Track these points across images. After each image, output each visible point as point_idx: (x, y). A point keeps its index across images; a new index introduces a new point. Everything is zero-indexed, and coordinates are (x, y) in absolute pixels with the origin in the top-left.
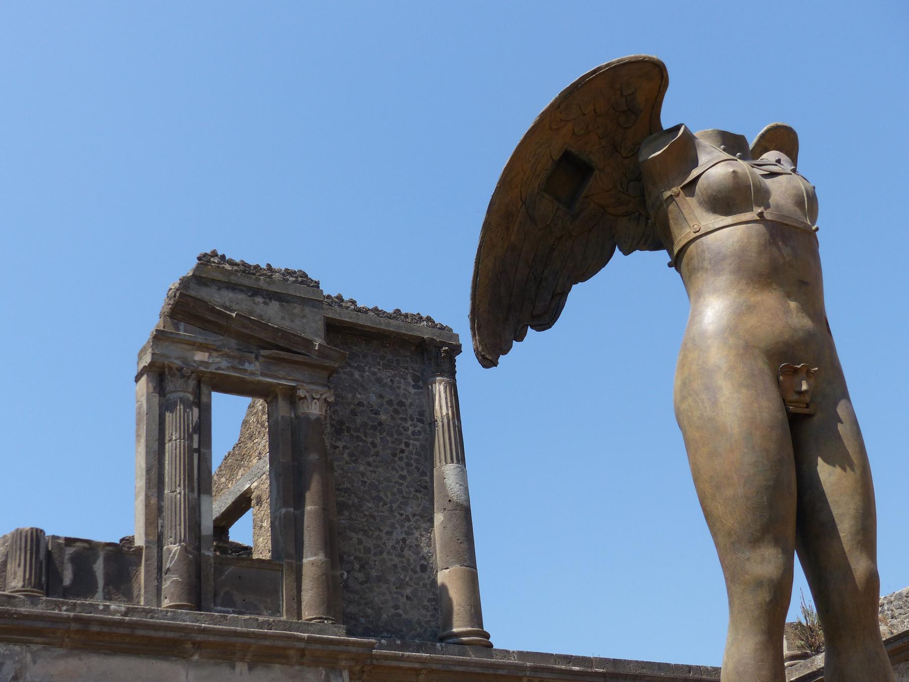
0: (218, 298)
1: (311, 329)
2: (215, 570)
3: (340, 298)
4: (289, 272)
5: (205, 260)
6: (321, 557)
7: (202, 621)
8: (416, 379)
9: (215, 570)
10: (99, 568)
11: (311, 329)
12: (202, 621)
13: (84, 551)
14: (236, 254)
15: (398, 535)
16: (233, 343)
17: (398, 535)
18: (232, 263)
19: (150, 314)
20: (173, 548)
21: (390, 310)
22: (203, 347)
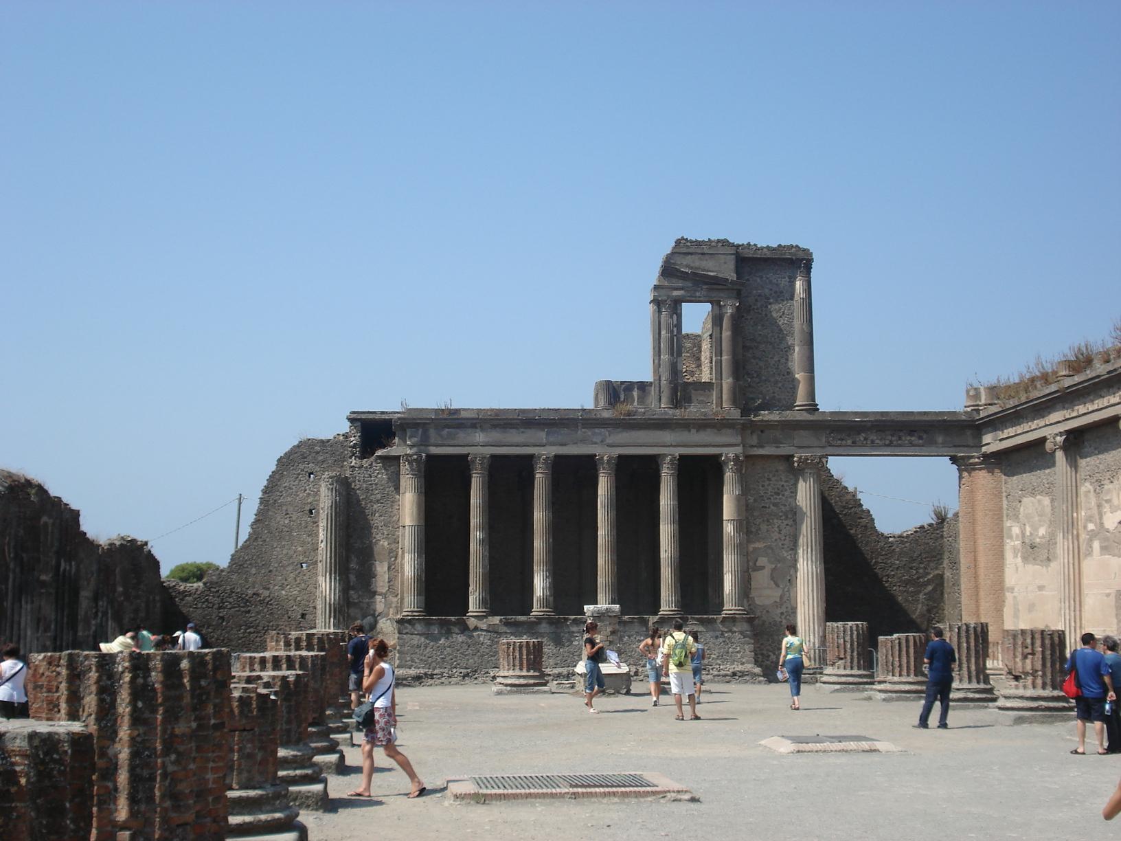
0: (684, 264)
1: (728, 271)
2: (682, 391)
3: (749, 244)
4: (719, 241)
5: (678, 242)
6: (730, 380)
7: (678, 412)
8: (790, 277)
9: (682, 391)
10: (635, 394)
11: (728, 271)
12: (678, 413)
13: (629, 386)
14: (692, 237)
15: (776, 359)
16: (689, 284)
17: (776, 359)
18: (691, 242)
19: (652, 275)
20: (663, 382)
21: (775, 246)
22: (677, 289)
